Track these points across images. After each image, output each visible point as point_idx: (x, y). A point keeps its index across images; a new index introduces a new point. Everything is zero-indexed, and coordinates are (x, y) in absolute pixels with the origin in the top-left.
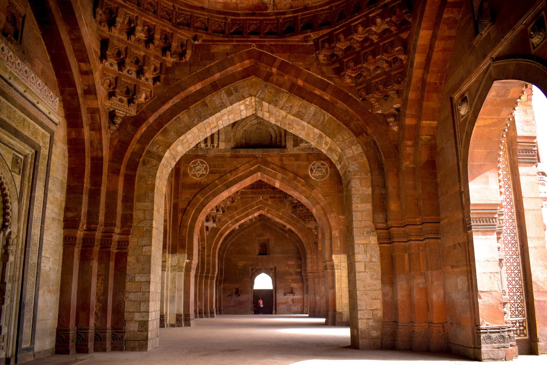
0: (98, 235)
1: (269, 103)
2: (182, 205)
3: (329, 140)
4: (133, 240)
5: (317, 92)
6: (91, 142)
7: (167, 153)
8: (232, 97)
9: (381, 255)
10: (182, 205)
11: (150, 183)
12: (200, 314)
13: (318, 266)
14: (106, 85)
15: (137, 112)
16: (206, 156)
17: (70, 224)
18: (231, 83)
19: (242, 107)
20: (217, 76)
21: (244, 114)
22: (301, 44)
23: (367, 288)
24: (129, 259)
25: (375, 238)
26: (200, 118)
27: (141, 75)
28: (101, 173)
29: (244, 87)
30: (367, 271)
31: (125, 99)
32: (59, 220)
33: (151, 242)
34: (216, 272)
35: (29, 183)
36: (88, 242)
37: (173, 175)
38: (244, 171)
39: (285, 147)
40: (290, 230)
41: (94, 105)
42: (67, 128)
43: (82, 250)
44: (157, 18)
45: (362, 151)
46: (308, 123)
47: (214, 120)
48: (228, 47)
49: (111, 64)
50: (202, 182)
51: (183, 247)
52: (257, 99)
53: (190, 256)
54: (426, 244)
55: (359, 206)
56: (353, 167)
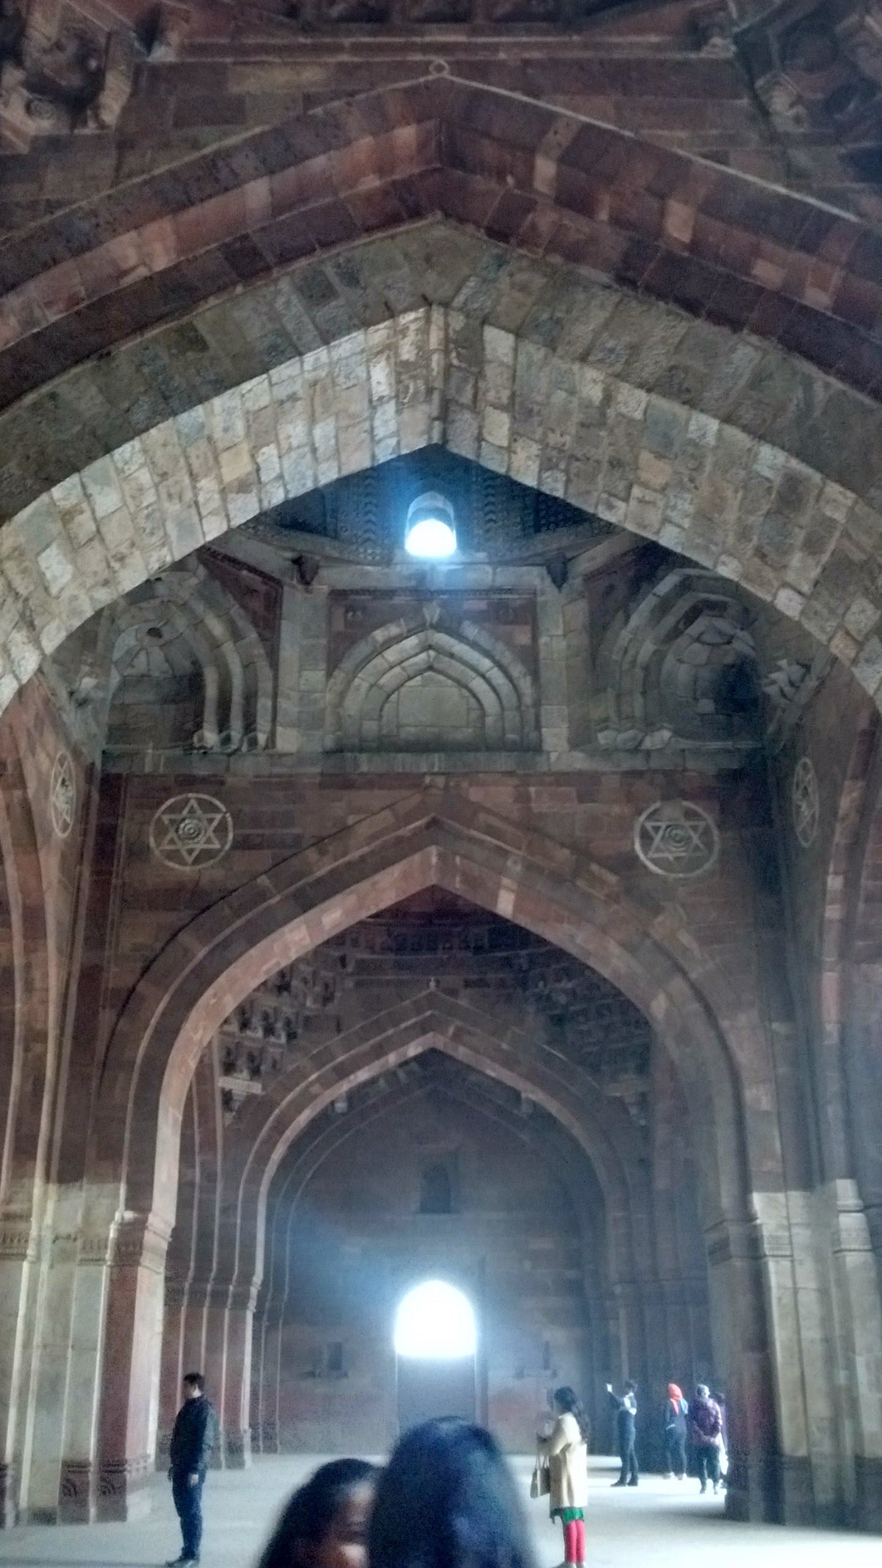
1: (519, 334)
2: (116, 977)
3: (837, 501)
8: (333, 309)
10: (117, 976)
16: (222, 783)
18: (326, 245)
19: (380, 377)
22: (678, 56)
26: (166, 398)
29: (391, 265)
34: (258, 1278)
37: (89, 854)
39: (537, 748)
47: (240, 427)
50: (204, 882)
51: (110, 1153)
53: (140, 1196)
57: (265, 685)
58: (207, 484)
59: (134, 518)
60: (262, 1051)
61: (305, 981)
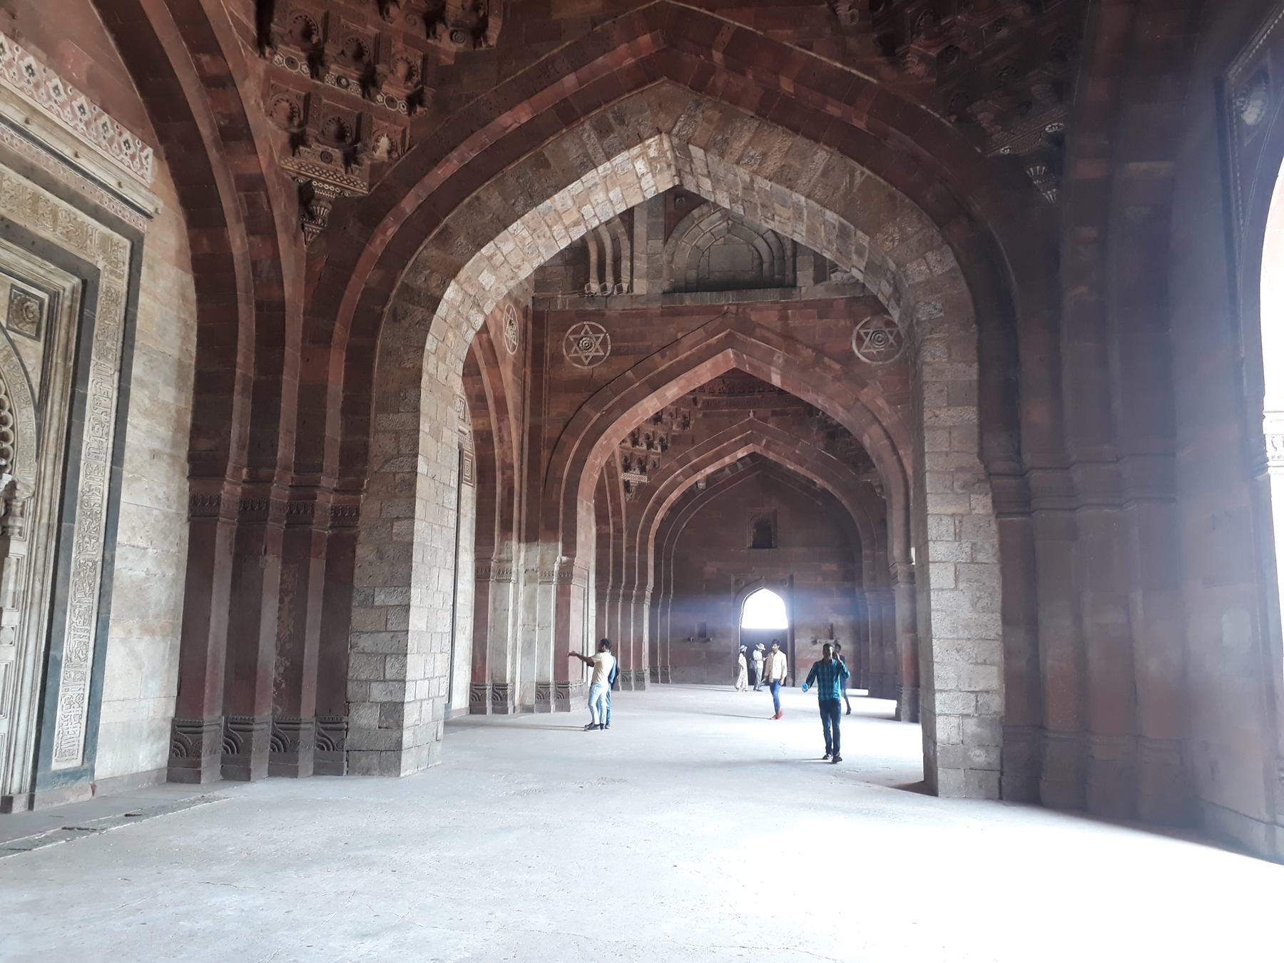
0: (279, 492)
3: (864, 240)
4: (369, 507)
5: (833, 110)
7: (449, 290)
8: (612, 139)
10: (548, 432)
11: (408, 365)
14: (282, 116)
15: (371, 186)
16: (603, 315)
17: (202, 464)
18: (606, 102)
19: (641, 166)
24: (360, 551)
25: (988, 500)
26: (531, 197)
27: (372, 90)
28: (281, 341)
30: (961, 586)
31: (337, 153)
32: (172, 456)
33: (413, 511)
35: (66, 359)
39: (794, 285)
40: (824, 490)
42: (189, 228)
43: (238, 531)
46: (808, 196)
47: (570, 203)
49: (287, 58)
52: (676, 141)
53: (570, 549)
55: (943, 414)
56: (928, 310)
57: (626, 252)
58: (558, 229)
59: (522, 250)
60: (646, 457)
61: (671, 415)
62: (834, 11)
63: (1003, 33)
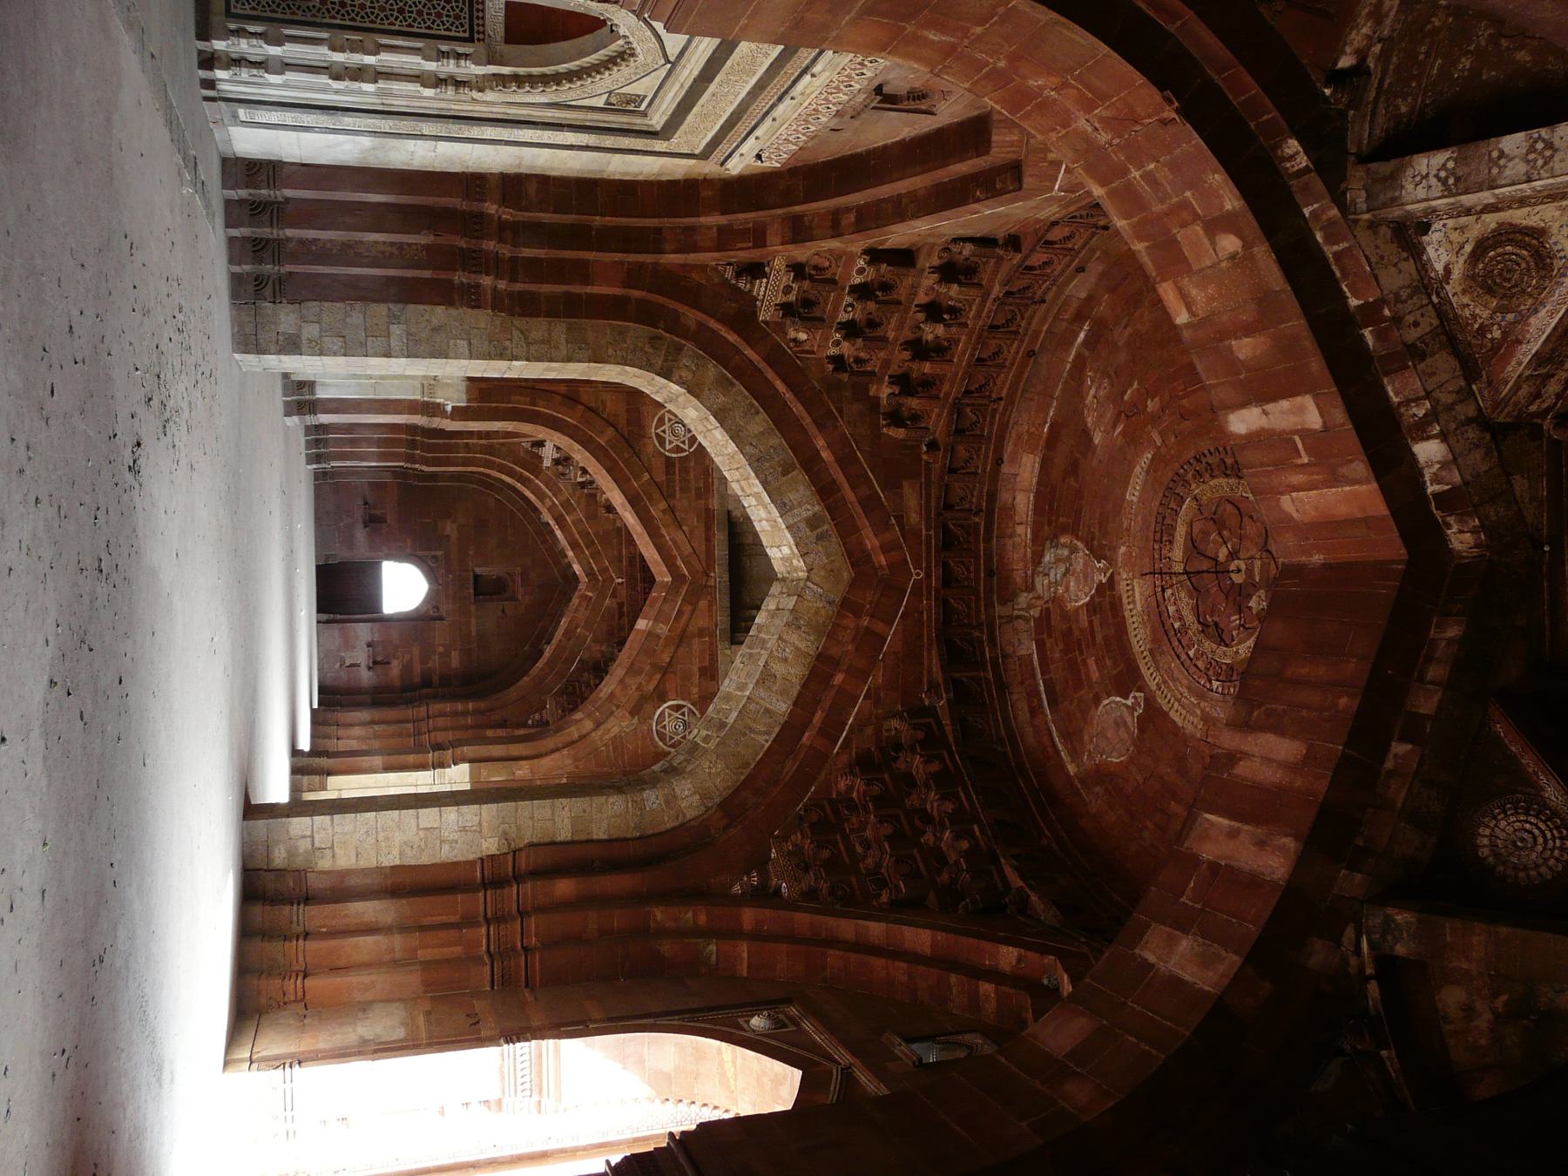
0: (490, 245)
1: (792, 611)
3: (711, 745)
4: (482, 319)
5: (818, 717)
6: (692, 229)
9: (455, 865)
11: (610, 351)
12: (318, 438)
13: (446, 729)
14: (816, 260)
15: (766, 323)
17: (512, 185)
19: (786, 550)
20: (850, 496)
21: (773, 553)
23: (381, 836)
24: (440, 309)
25: (494, 850)
29: (828, 555)
30: (421, 833)
31: (792, 297)
34: (425, 468)
36: (474, 224)
38: (675, 543)
40: (541, 653)
41: (773, 238)
44: (969, 365)
45: (689, 817)
48: (914, 518)
54: (481, 958)
55: (566, 813)
56: (652, 798)
62: (894, 716)
63: (859, 849)
